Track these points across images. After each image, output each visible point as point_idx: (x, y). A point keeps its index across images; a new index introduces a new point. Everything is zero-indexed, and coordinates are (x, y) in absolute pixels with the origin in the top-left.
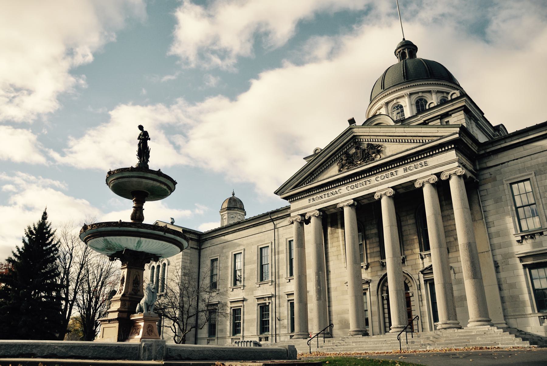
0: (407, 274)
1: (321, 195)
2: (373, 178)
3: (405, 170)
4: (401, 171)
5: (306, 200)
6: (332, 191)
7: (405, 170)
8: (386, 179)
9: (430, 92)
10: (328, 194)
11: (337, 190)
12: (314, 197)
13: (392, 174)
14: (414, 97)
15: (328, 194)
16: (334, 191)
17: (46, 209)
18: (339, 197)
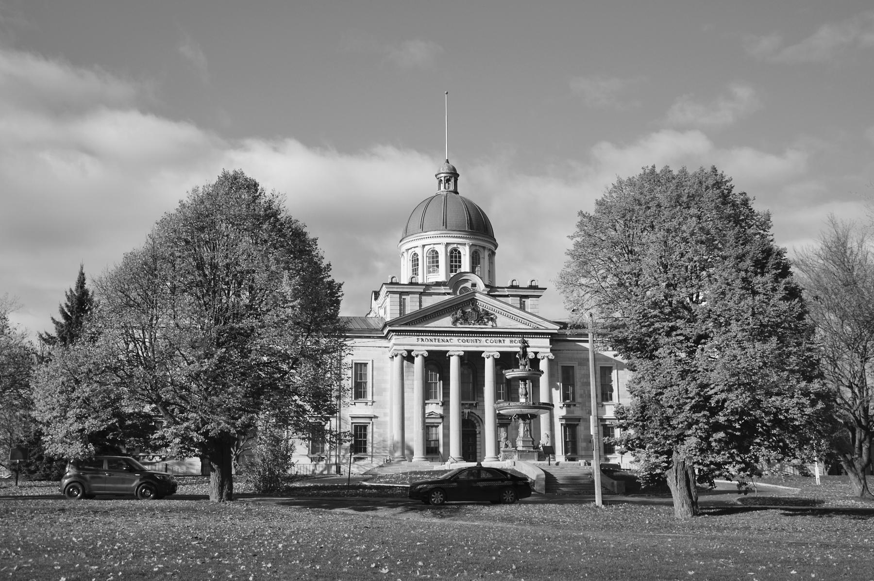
0: (478, 416)
1: (431, 338)
2: (484, 339)
3: (511, 342)
4: (507, 340)
5: (416, 337)
6: (443, 338)
7: (511, 342)
8: (494, 344)
9: (484, 248)
10: (438, 340)
11: (448, 338)
12: (424, 338)
13: (500, 341)
14: (474, 248)
15: (438, 340)
16: (445, 338)
17: (82, 268)
18: (450, 346)
